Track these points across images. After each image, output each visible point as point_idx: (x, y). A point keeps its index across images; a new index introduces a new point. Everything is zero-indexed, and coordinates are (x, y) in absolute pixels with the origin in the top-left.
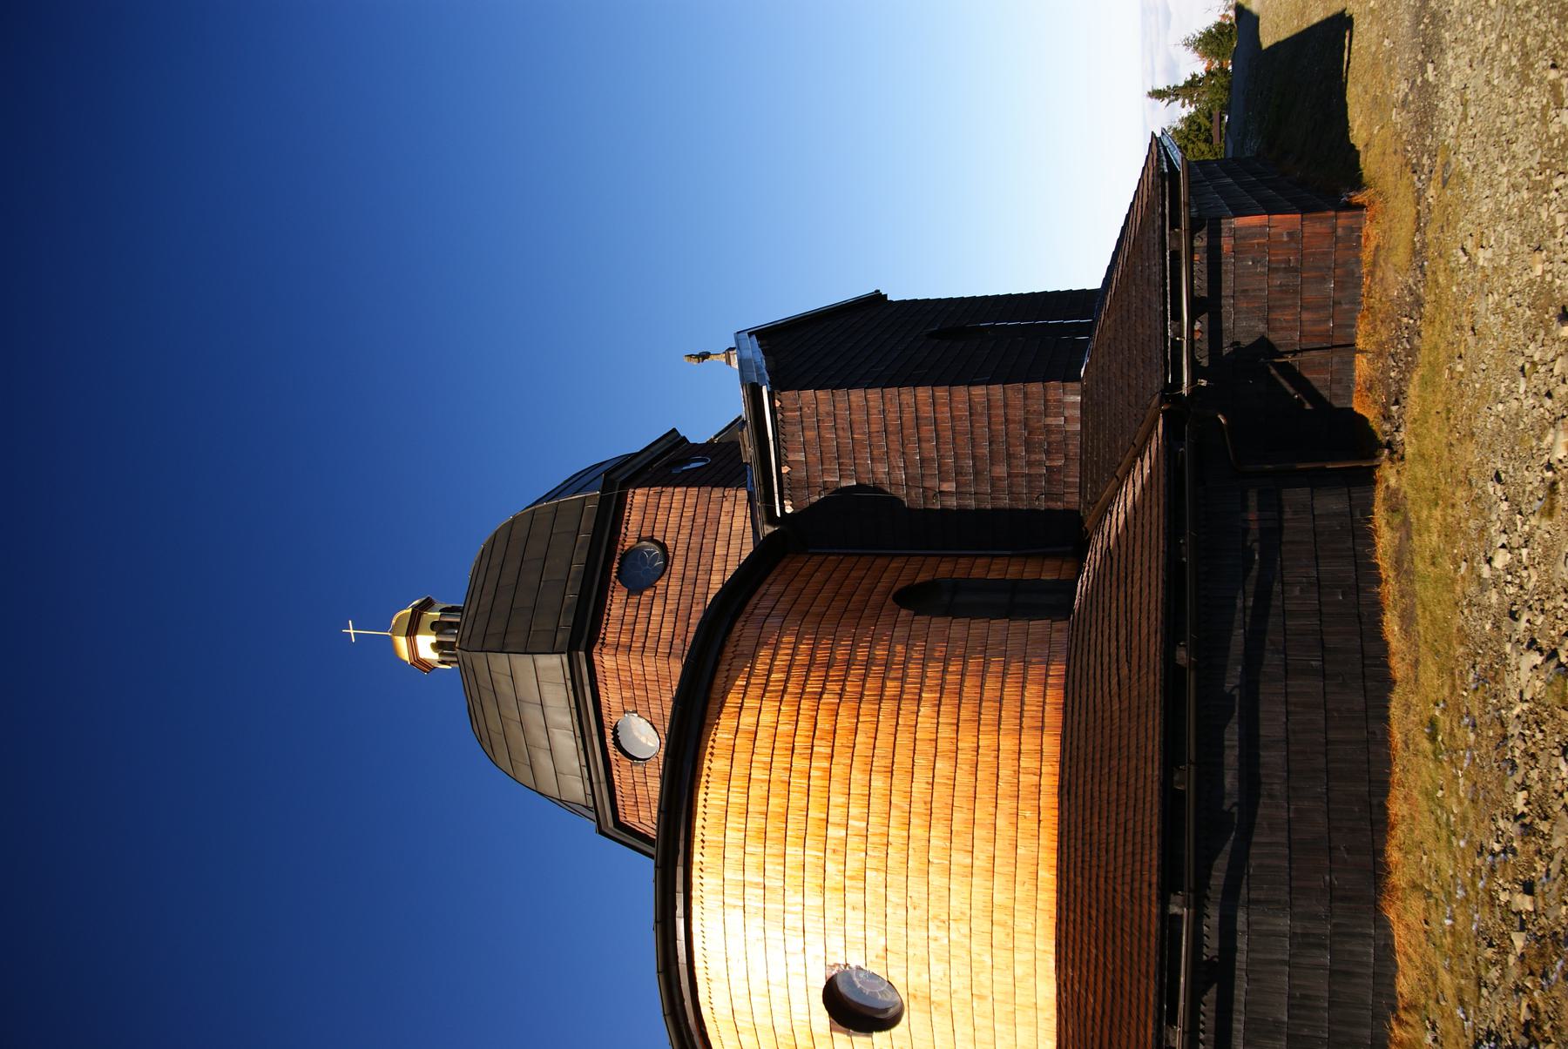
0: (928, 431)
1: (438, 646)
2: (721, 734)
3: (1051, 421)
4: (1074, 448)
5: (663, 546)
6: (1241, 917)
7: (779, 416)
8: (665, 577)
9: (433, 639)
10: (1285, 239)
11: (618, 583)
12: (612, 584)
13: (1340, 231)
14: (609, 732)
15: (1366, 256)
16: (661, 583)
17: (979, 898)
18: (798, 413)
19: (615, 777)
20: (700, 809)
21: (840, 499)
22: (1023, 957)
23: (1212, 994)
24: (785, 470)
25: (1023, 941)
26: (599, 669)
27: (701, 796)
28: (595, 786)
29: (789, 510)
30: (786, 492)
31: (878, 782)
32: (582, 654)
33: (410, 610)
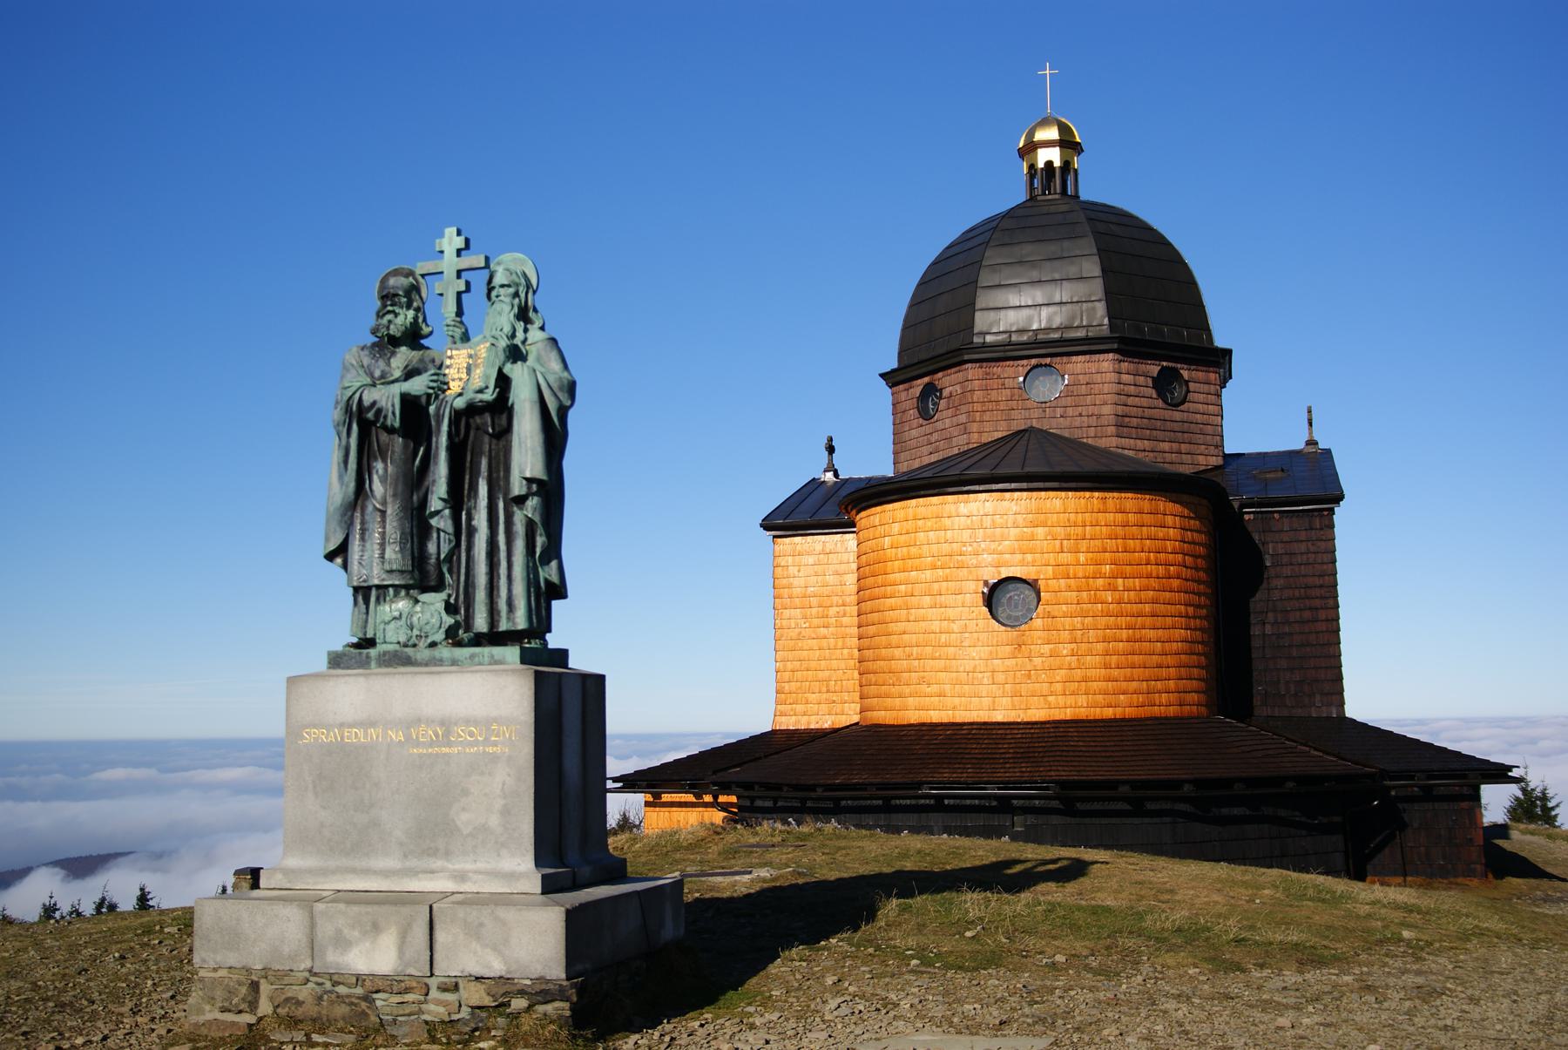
0: (1307, 615)
1: (1049, 164)
2: (1162, 504)
3: (1318, 697)
4: (1299, 712)
5: (1183, 402)
6: (1168, 819)
7: (1316, 514)
8: (1165, 406)
9: (1057, 164)
10: (1469, 837)
11: (1159, 368)
12: (1158, 363)
13: (1473, 866)
14: (1048, 360)
15: (1460, 880)
16: (1160, 403)
17: (1092, 673)
18: (1318, 527)
19: (1008, 363)
20: (1123, 495)
21: (1256, 555)
22: (1061, 700)
23: (1126, 807)
24: (1276, 516)
25: (1070, 700)
26: (1102, 356)
27: (1130, 495)
28: (1002, 348)
29: (1246, 517)
30: (1260, 516)
31: (1147, 608)
32: (1115, 346)
33: (1078, 140)
